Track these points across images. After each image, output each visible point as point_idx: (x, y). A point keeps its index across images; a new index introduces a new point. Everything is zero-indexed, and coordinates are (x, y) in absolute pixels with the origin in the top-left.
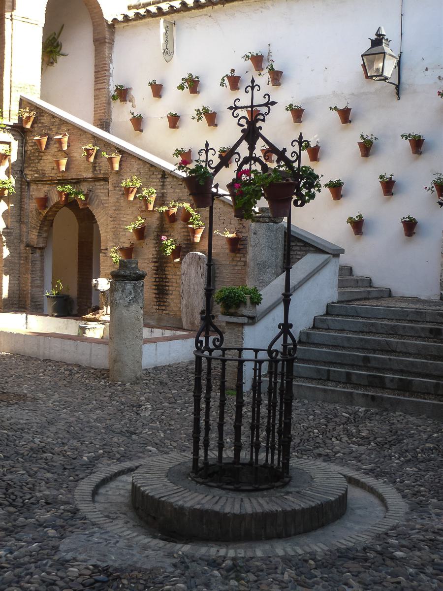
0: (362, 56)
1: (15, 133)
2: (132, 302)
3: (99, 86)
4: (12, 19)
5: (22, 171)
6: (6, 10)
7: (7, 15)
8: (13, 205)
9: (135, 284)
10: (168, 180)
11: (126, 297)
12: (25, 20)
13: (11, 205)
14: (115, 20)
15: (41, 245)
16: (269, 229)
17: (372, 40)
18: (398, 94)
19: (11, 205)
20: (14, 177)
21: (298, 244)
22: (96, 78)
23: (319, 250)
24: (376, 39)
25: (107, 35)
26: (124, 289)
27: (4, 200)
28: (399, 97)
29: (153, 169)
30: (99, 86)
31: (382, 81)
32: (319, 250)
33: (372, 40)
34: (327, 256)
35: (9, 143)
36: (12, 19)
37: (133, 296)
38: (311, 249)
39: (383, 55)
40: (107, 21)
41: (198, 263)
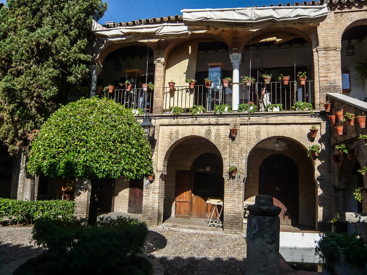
1: (322, 117)
2: (256, 236)
4: (317, 52)
5: (329, 140)
6: (313, 47)
7: (314, 50)
8: (324, 161)
9: (259, 219)
11: (252, 231)
12: (326, 49)
13: (322, 162)
15: (342, 187)
19: (322, 162)
20: (324, 144)
27: (318, 159)
35: (320, 123)
36: (317, 52)
37: (257, 230)
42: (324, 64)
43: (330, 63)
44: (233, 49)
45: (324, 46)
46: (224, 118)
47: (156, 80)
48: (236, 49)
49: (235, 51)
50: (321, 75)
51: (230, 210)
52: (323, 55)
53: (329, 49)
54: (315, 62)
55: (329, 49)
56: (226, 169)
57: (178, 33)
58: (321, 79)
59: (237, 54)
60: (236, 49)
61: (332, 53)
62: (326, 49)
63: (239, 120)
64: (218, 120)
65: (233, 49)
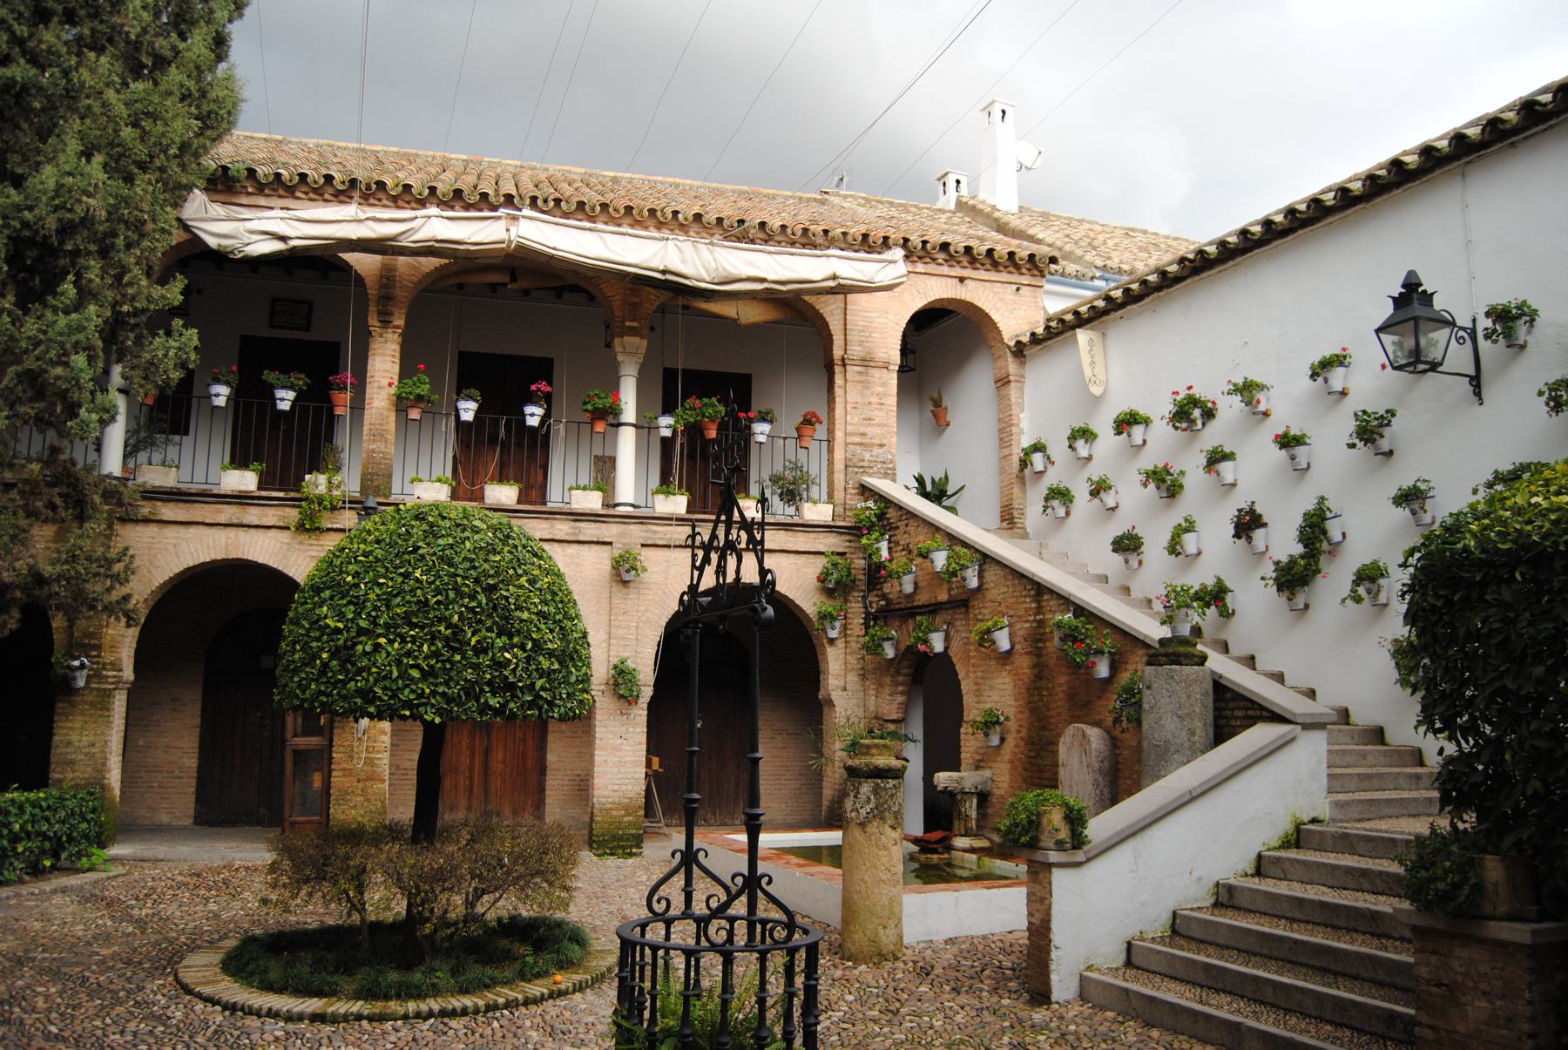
0: (1378, 331)
3: (1006, 451)
9: (877, 785)
10: (1045, 597)
14: (1018, 343)
16: (1172, 677)
17: (1393, 298)
18: (1478, 393)
21: (1242, 704)
22: (1001, 439)
23: (1277, 718)
24: (1401, 294)
26: (858, 793)
28: (1480, 399)
29: (1025, 581)
30: (1006, 451)
31: (1430, 374)
32: (1277, 718)
33: (1393, 298)
38: (1264, 714)
39: (1412, 322)
40: (1009, 347)
41: (1081, 745)
42: (859, 400)
43: (874, 400)
44: (628, 324)
45: (862, 354)
46: (598, 525)
47: (376, 385)
48: (635, 324)
49: (633, 332)
50: (849, 429)
51: (610, 787)
52: (856, 378)
53: (872, 364)
55: (872, 364)
56: (600, 670)
57: (461, 247)
58: (850, 439)
59: (636, 340)
60: (635, 324)
61: (876, 373)
62: (867, 362)
63: (637, 533)
64: (579, 528)
65: (628, 324)
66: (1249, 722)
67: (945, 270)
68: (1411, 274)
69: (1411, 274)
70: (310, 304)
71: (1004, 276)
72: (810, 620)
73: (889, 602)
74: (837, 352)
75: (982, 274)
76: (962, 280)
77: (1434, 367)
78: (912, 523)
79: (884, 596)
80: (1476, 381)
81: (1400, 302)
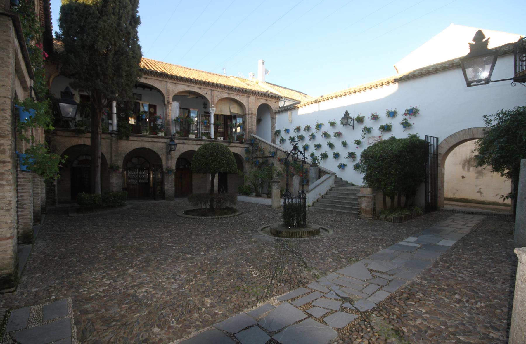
18: (353, 128)
25: (274, 116)
32: (329, 174)
34: (330, 175)
49: (213, 107)
54: (247, 119)
62: (252, 114)
66: (324, 174)
67: (264, 98)
68: (347, 111)
69: (347, 111)
70: (141, 95)
71: (274, 100)
72: (243, 158)
73: (257, 156)
74: (247, 112)
75: (270, 99)
76: (267, 100)
77: (349, 125)
78: (263, 143)
79: (256, 155)
80: (353, 127)
81: (345, 115)
